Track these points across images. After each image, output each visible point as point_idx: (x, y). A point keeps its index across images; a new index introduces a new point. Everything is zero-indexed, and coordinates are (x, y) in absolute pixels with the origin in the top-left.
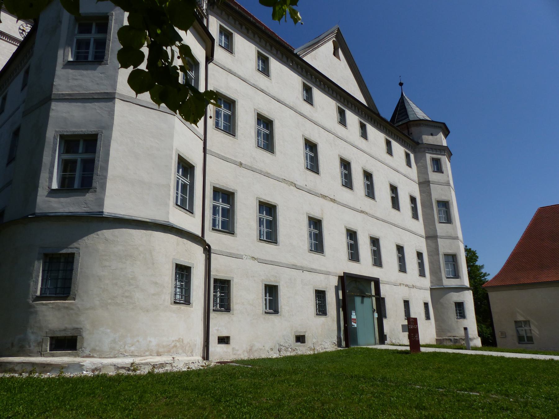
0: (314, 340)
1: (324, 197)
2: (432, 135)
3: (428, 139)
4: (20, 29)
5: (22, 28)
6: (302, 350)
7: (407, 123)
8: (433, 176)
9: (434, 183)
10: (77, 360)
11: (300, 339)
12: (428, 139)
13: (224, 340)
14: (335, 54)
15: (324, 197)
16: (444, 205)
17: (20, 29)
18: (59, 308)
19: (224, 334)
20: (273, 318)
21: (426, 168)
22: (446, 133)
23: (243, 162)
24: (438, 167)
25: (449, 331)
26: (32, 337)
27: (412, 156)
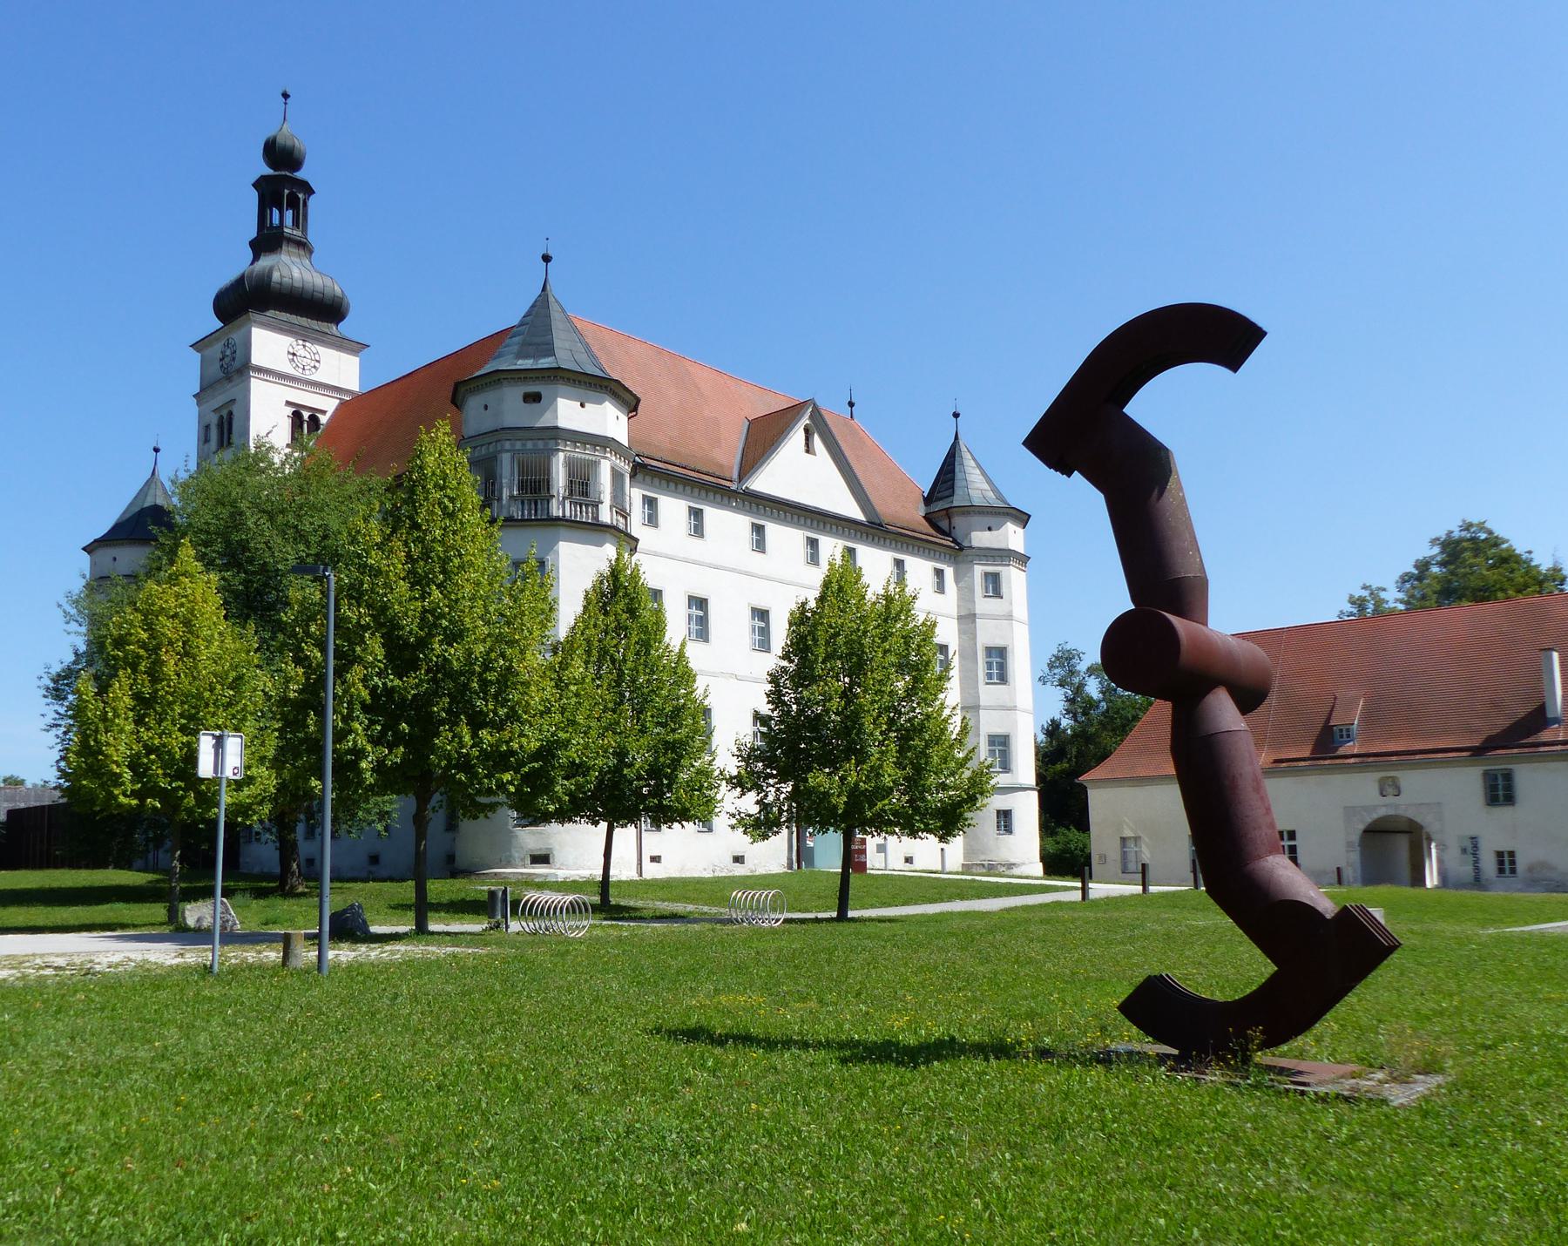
0: (756, 861)
2: (990, 529)
3: (981, 538)
4: (289, 353)
5: (291, 351)
6: (739, 870)
7: (947, 509)
8: (984, 605)
9: (984, 617)
10: (553, 871)
12: (981, 539)
13: (655, 859)
14: (809, 449)
16: (998, 657)
17: (289, 353)
18: (533, 833)
21: (972, 591)
22: (1022, 518)
24: (994, 585)
25: (983, 853)
26: (516, 855)
27: (949, 572)
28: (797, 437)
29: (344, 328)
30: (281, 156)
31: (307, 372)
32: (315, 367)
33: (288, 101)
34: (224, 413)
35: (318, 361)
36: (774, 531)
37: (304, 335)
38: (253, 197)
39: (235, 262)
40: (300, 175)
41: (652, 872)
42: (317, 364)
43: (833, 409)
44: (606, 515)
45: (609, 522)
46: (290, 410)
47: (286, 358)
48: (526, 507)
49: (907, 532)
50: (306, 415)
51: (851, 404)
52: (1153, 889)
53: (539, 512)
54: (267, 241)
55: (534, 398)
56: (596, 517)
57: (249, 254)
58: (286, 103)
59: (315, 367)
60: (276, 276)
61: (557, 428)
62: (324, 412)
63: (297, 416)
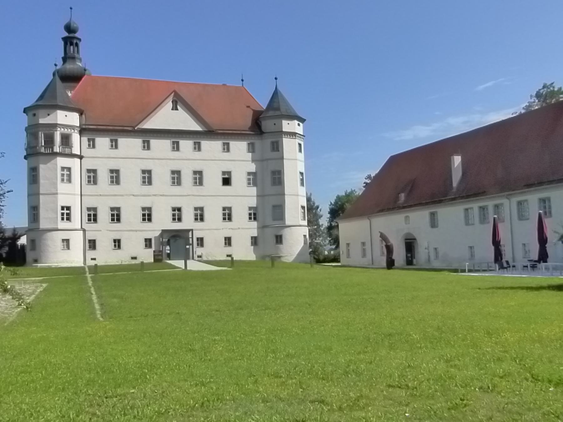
6: (134, 262)
11: (134, 258)
14: (175, 108)
19: (93, 257)
20: (119, 251)
23: (101, 194)
30: (69, 29)
36: (154, 143)
40: (76, 35)
48: (48, 149)
51: (242, 80)
53: (48, 151)
56: (53, 150)
58: (71, 11)
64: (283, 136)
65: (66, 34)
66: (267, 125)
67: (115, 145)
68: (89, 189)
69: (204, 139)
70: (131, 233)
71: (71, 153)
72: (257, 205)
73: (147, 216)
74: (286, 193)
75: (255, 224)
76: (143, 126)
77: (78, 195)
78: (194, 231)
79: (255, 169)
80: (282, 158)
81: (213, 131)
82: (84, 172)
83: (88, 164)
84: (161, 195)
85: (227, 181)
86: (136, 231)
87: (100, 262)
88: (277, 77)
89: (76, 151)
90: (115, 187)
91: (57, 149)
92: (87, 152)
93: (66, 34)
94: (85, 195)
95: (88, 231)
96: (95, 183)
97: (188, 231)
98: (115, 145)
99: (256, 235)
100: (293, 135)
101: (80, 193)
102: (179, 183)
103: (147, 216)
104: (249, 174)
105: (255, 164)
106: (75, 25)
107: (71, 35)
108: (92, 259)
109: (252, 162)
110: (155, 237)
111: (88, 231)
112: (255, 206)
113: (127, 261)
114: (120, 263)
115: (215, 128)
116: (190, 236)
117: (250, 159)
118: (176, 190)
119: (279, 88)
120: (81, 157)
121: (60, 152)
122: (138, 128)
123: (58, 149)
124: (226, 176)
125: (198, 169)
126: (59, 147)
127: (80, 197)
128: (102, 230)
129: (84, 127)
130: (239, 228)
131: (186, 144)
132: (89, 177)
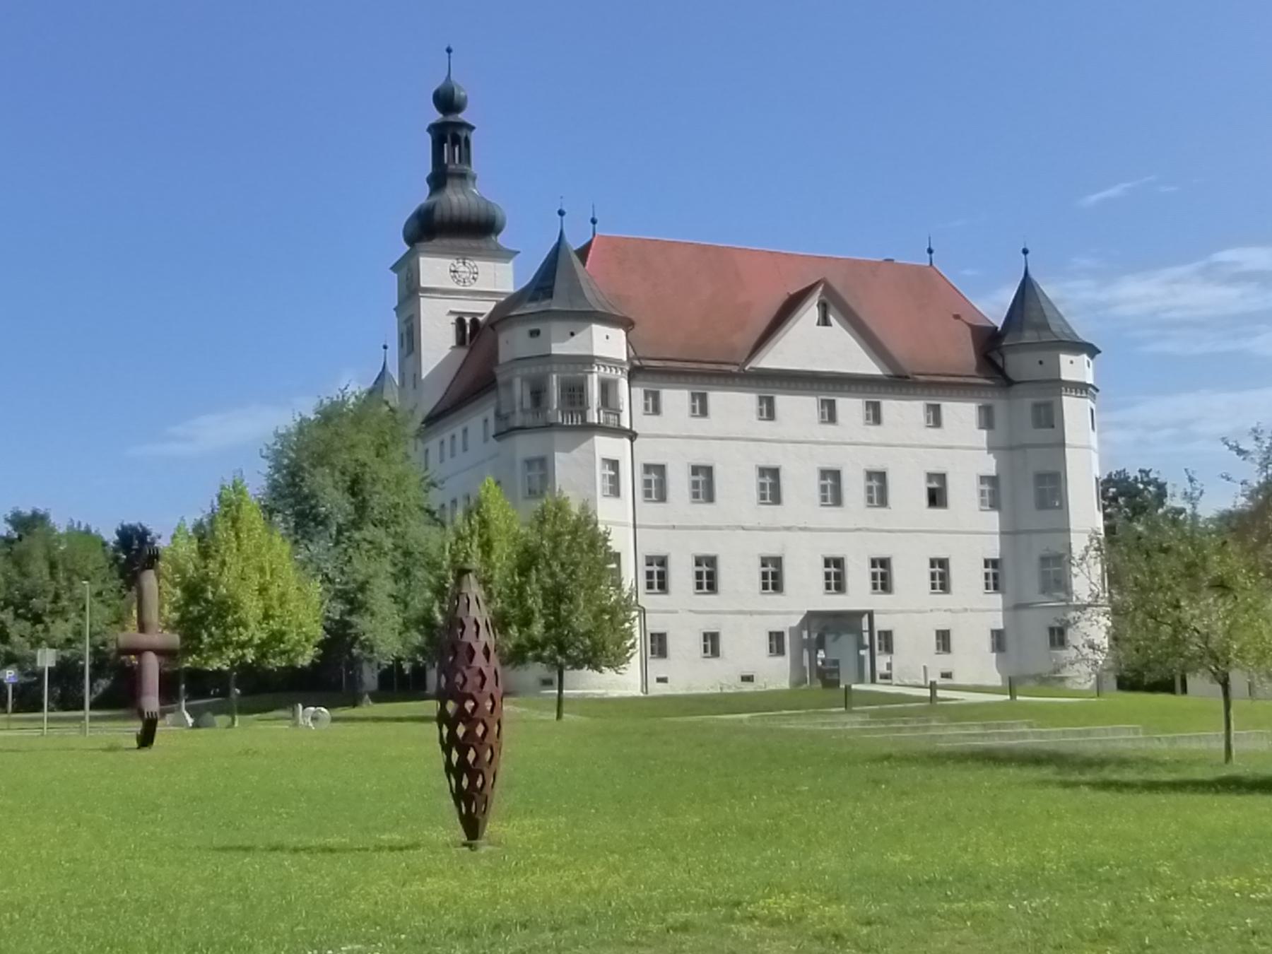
1: (788, 529)
5: (453, 269)
6: (748, 688)
11: (748, 679)
13: (662, 680)
14: (825, 321)
15: (788, 529)
17: (451, 271)
19: (662, 675)
20: (714, 661)
23: (675, 524)
28: (810, 311)
29: (502, 239)
30: (446, 101)
31: (467, 284)
32: (474, 278)
33: (452, 54)
34: (409, 324)
35: (477, 273)
36: (784, 402)
37: (463, 255)
38: (428, 139)
39: (420, 195)
40: (462, 117)
41: (657, 689)
42: (475, 276)
43: (837, 285)
44: (594, 417)
45: (596, 421)
46: (453, 319)
47: (449, 275)
49: (944, 379)
50: (468, 320)
51: (930, 251)
52: (1018, 698)
54: (439, 180)
55: (535, 333)
56: (584, 419)
57: (427, 189)
58: (449, 57)
59: (474, 278)
60: (437, 213)
61: (549, 355)
62: (482, 314)
63: (460, 323)
64: (1061, 391)
65: (437, 116)
66: (1019, 364)
67: (701, 408)
68: (651, 512)
69: (951, 398)
70: (741, 617)
71: (619, 425)
72: (1000, 555)
73: (773, 577)
74: (1072, 527)
75: (997, 600)
76: (759, 363)
77: (626, 525)
78: (875, 616)
79: (994, 469)
80: (1062, 444)
81: (907, 377)
82: (639, 470)
83: (649, 451)
84: (801, 529)
85: (936, 498)
86: (751, 613)
87: (676, 687)
88: (1029, 248)
89: (625, 424)
90: (705, 508)
91: (594, 417)
92: (643, 424)
93: (437, 116)
94: (642, 527)
95: (651, 612)
96: (662, 498)
97: (860, 614)
98: (701, 408)
99: (1001, 626)
100: (1081, 388)
101: (631, 522)
102: (838, 501)
103: (773, 577)
104: (983, 479)
105: (995, 457)
106: (462, 94)
107: (451, 118)
108: (660, 680)
109: (989, 453)
110: (791, 629)
111: (651, 612)
112: (998, 557)
113: (733, 685)
114: (719, 691)
115: (908, 368)
116: (865, 627)
117: (985, 445)
118: (832, 516)
119: (1031, 272)
120: (632, 436)
121: (599, 423)
122: (751, 368)
123: (596, 415)
124: (935, 485)
125: (877, 466)
126: (598, 411)
127: (631, 530)
128: (680, 611)
129: (637, 363)
130: (966, 610)
131: (850, 407)
132: (648, 483)
